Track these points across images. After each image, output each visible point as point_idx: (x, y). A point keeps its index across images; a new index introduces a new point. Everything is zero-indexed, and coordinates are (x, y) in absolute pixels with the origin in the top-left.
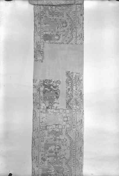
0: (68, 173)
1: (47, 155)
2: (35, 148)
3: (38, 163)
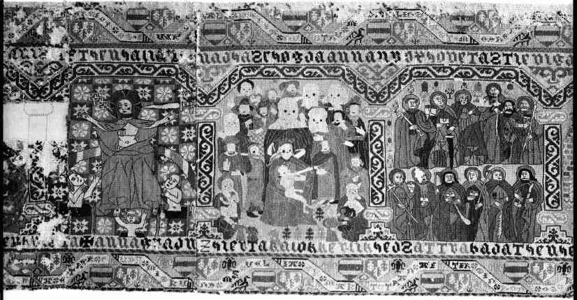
0: (431, 90)
1: (332, 212)
2: (292, 275)
3: (380, 262)
